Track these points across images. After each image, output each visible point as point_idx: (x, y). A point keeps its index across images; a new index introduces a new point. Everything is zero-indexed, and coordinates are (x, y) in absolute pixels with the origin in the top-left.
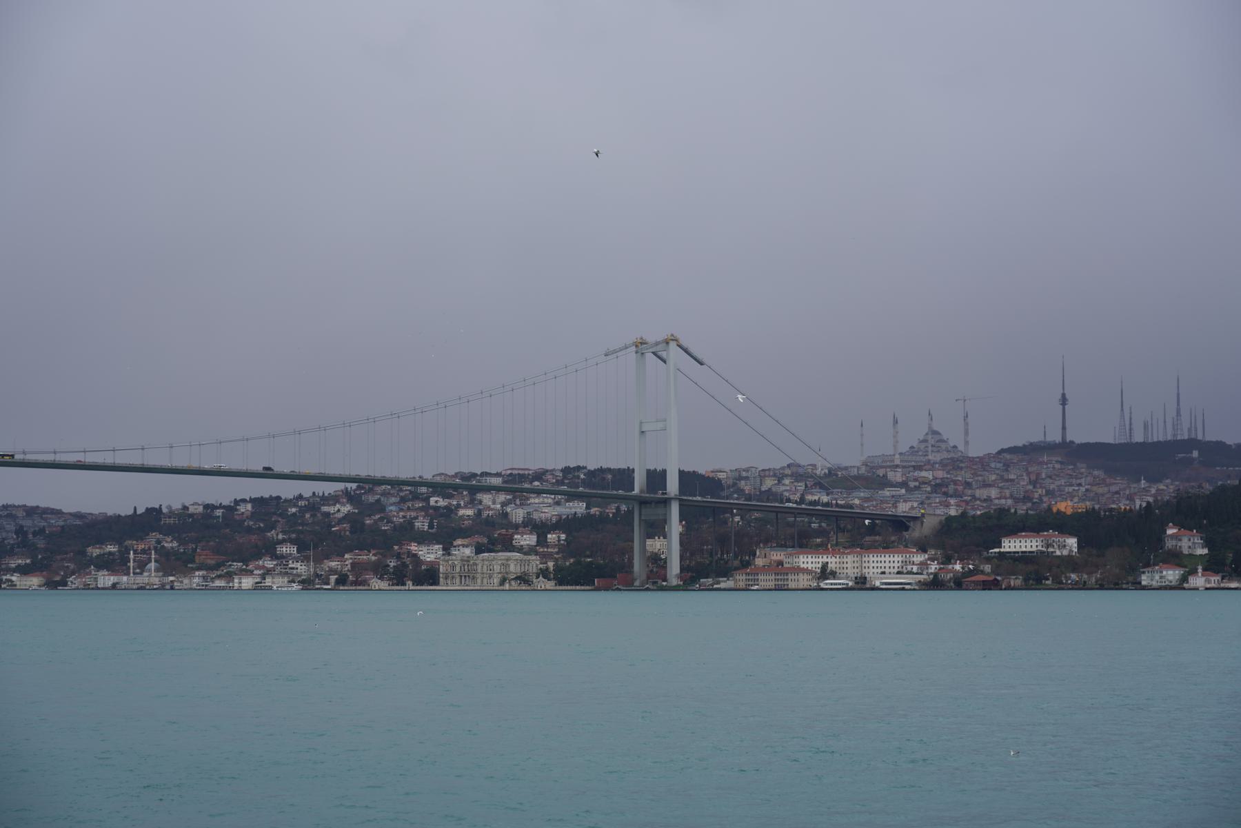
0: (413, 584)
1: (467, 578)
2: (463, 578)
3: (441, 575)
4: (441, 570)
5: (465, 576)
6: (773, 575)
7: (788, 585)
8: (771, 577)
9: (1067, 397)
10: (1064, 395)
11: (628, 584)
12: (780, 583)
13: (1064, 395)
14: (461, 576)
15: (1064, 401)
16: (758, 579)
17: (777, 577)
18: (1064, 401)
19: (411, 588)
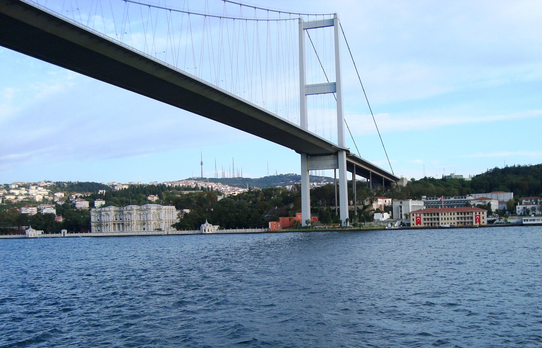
0: (68, 233)
1: (121, 226)
2: (117, 226)
3: (92, 224)
4: (93, 219)
6: (456, 214)
7: (439, 223)
8: (452, 216)
10: (202, 161)
12: (433, 221)
14: (114, 224)
15: (202, 164)
16: (438, 219)
17: (433, 217)
18: (202, 164)
19: (66, 235)
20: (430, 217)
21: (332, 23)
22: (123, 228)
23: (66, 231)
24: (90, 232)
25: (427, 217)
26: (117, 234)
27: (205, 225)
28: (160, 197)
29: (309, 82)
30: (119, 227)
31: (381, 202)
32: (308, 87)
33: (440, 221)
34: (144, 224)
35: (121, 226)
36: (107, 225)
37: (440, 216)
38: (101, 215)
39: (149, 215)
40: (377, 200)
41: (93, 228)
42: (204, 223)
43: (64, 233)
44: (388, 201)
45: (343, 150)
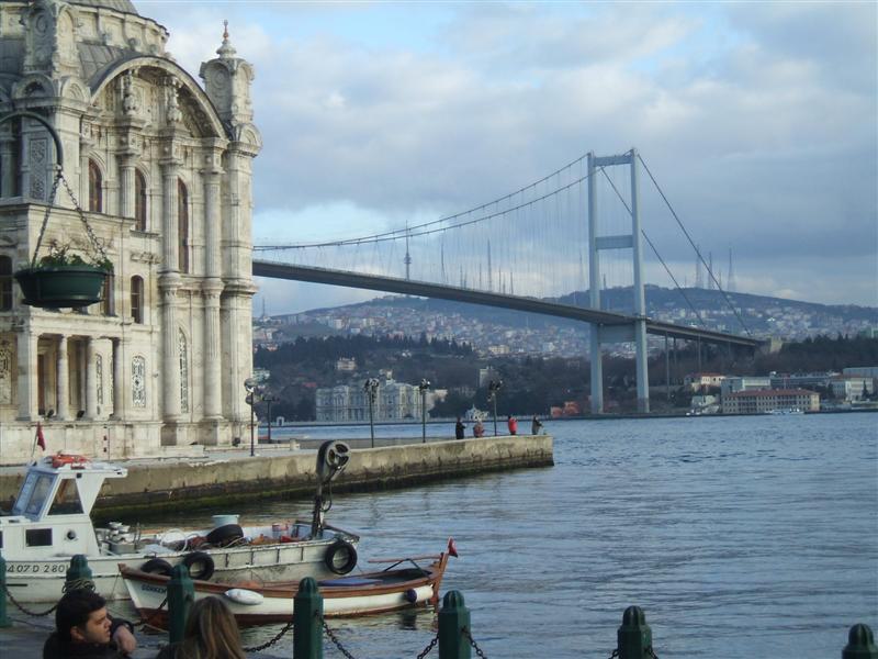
1: (359, 413)
4: (319, 402)
5: (356, 410)
8: (772, 401)
9: (411, 256)
10: (408, 254)
11: (584, 414)
13: (408, 254)
14: (350, 410)
20: (745, 401)
21: (629, 158)
22: (362, 415)
23: (283, 419)
24: (314, 419)
25: (742, 401)
26: (355, 422)
27: (472, 411)
28: (360, 363)
29: (600, 233)
30: (356, 414)
31: (706, 381)
32: (597, 239)
33: (758, 407)
34: (390, 410)
35: (359, 413)
36: (340, 411)
37: (758, 401)
38: (331, 399)
39: (397, 398)
40: (699, 379)
41: (319, 415)
42: (470, 408)
43: (280, 421)
44: (718, 380)
45: (640, 320)
